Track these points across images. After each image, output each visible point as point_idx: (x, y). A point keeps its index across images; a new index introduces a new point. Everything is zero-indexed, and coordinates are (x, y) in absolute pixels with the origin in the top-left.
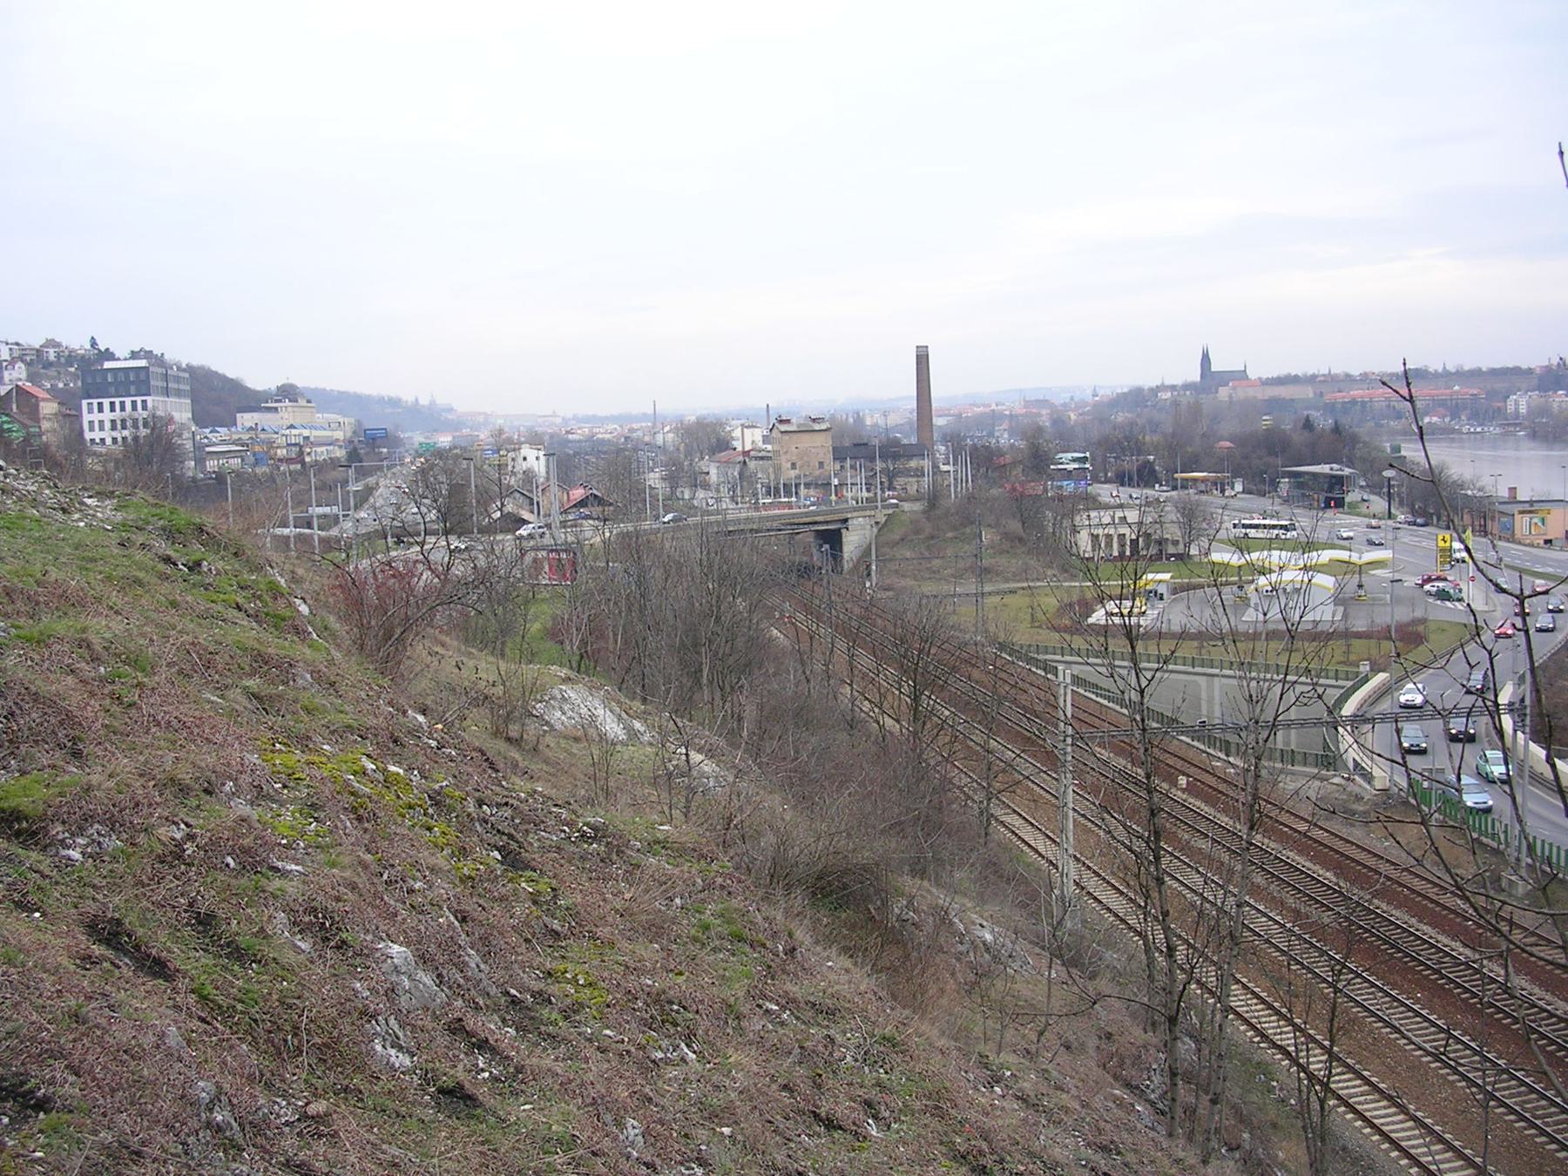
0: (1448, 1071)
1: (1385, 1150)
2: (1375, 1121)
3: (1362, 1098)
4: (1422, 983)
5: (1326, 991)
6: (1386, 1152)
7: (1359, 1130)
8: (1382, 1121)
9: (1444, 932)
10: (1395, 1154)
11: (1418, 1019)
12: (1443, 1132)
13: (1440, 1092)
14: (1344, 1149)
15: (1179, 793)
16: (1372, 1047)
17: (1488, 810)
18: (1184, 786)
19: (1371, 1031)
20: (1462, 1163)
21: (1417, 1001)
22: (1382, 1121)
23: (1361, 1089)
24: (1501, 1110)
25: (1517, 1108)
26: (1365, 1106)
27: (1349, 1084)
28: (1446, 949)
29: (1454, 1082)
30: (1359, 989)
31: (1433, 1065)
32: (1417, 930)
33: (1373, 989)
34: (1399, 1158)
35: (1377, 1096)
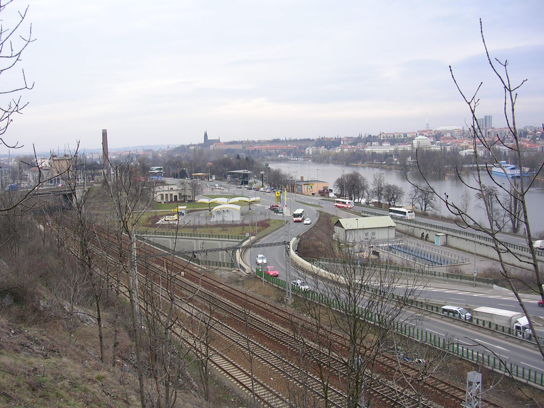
0: (261, 360)
1: (238, 386)
2: (236, 377)
3: (232, 370)
4: (256, 333)
5: (224, 338)
6: (239, 386)
7: (230, 380)
8: (238, 377)
9: (264, 317)
10: (241, 387)
11: (253, 344)
12: (257, 379)
13: (258, 367)
14: (225, 386)
15: (182, 278)
16: (237, 354)
17: (277, 276)
18: (183, 275)
19: (237, 349)
20: (262, 387)
21: (253, 339)
22: (238, 377)
23: (232, 367)
24: (277, 370)
25: (282, 369)
26: (233, 373)
27: (228, 366)
28: (264, 322)
29: (262, 363)
30: (235, 336)
31: (256, 358)
32: (255, 317)
33: (239, 336)
34: (242, 388)
35: (237, 369)
